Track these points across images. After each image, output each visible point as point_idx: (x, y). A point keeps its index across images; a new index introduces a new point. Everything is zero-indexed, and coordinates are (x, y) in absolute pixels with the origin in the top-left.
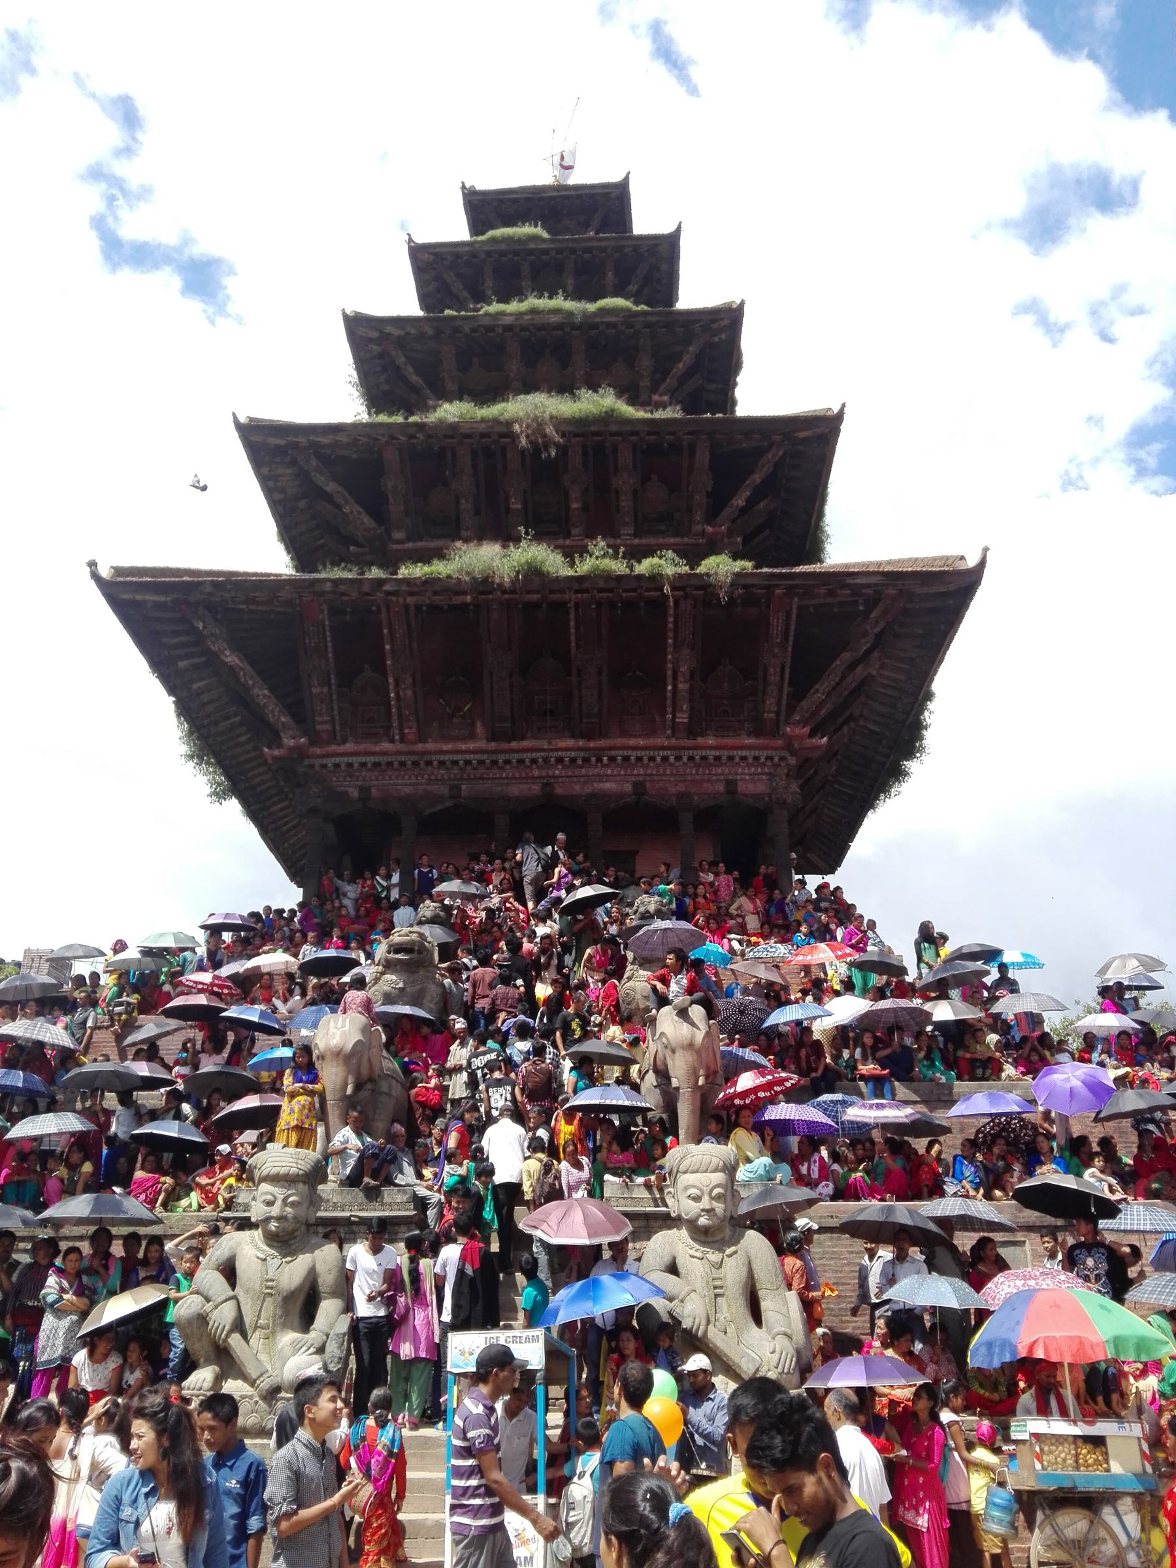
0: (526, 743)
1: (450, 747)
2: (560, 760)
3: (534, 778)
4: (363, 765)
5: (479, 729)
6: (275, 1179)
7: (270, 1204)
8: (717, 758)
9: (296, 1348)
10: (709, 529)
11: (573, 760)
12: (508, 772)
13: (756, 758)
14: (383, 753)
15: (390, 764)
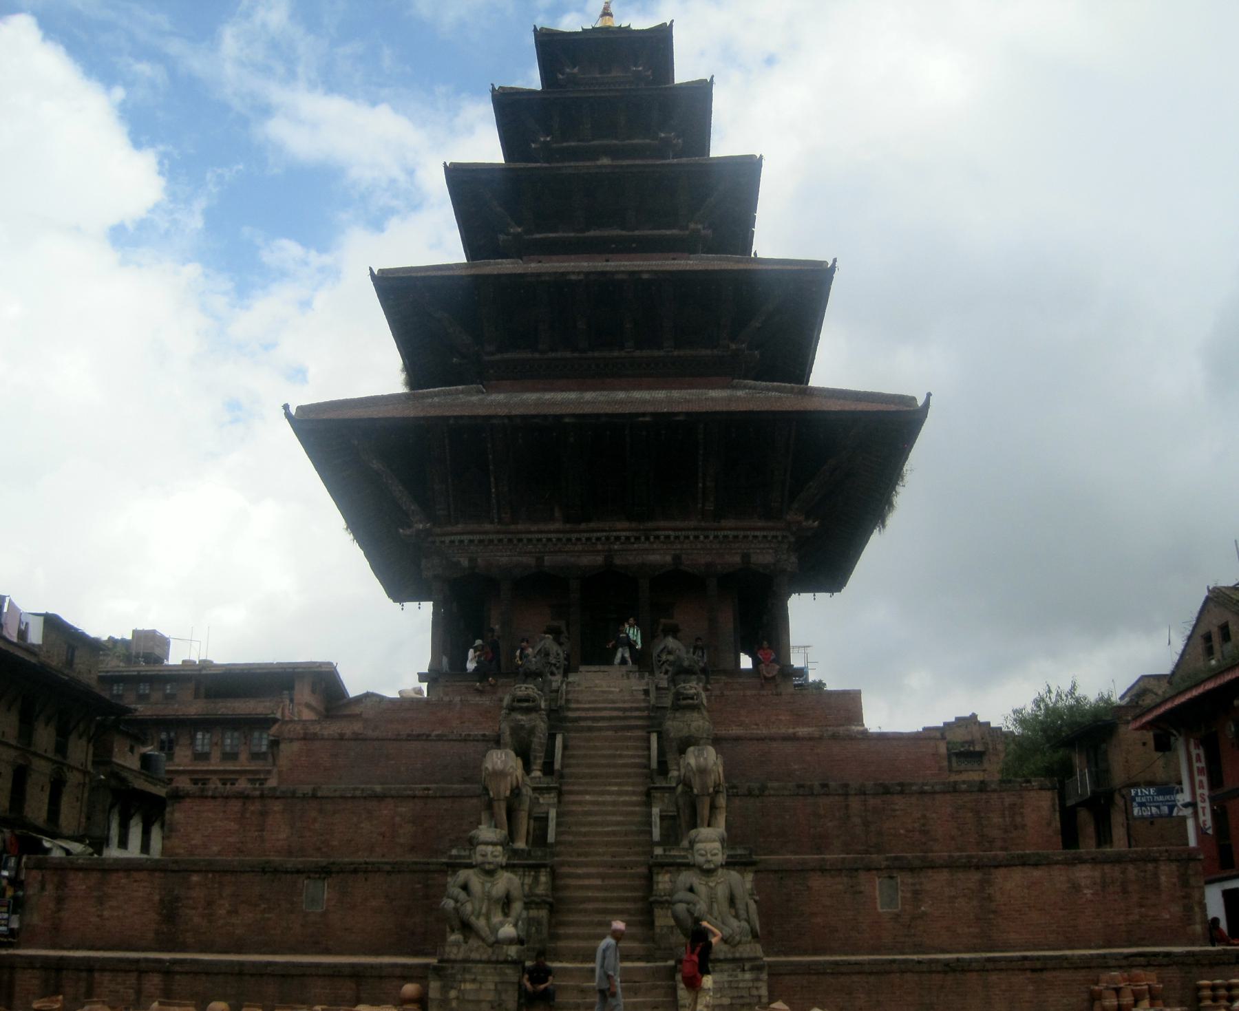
0: (592, 525)
1: (534, 528)
2: (617, 538)
3: (599, 551)
4: (471, 541)
5: (557, 514)
6: (487, 843)
7: (483, 856)
8: (736, 537)
9: (502, 924)
10: (733, 346)
11: (628, 538)
12: (579, 547)
13: (765, 537)
14: (486, 533)
15: (491, 541)
